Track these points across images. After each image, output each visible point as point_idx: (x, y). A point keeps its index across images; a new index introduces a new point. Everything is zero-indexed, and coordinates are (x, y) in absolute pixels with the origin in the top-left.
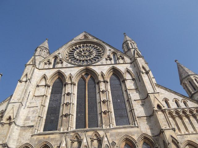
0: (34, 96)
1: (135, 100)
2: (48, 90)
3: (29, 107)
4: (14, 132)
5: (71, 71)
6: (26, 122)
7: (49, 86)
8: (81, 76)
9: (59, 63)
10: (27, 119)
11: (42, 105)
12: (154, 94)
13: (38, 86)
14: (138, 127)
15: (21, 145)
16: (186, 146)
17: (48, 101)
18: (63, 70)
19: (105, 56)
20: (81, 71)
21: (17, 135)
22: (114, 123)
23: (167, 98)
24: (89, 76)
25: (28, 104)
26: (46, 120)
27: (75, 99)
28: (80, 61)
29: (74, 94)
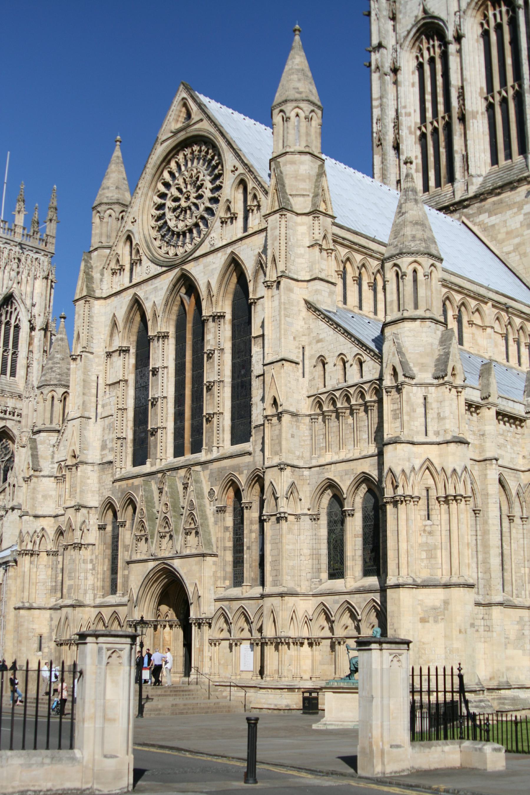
0: (107, 385)
1: (258, 376)
2: (126, 362)
3: (103, 416)
4: (88, 478)
5: (156, 289)
6: (104, 452)
7: (126, 351)
8: (178, 298)
9: (136, 263)
10: (104, 447)
11: (119, 409)
12: (272, 366)
13: (109, 355)
14: (250, 454)
15: (104, 499)
16: (325, 489)
17: (131, 392)
18: (141, 292)
19: (220, 211)
20: (175, 286)
21: (96, 480)
22: (223, 441)
23: (326, 356)
24: (193, 299)
25: (100, 410)
26: (134, 440)
27: (168, 381)
28: (178, 234)
29: (167, 367)
